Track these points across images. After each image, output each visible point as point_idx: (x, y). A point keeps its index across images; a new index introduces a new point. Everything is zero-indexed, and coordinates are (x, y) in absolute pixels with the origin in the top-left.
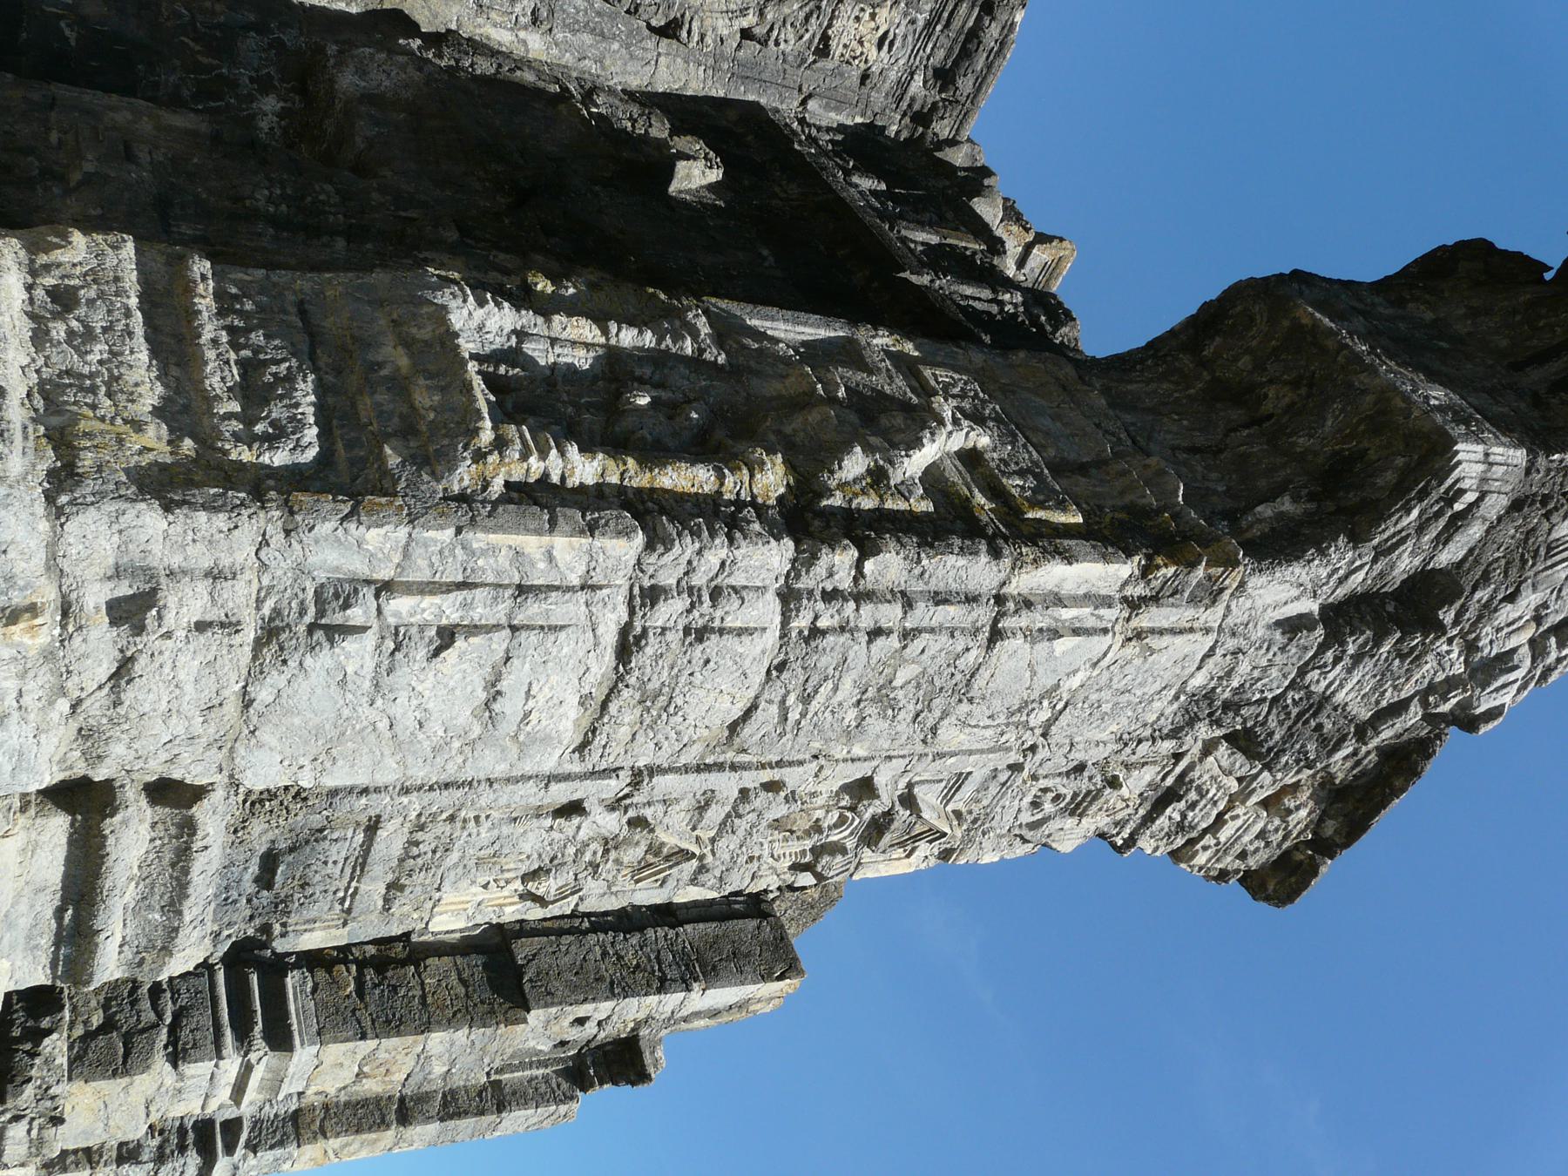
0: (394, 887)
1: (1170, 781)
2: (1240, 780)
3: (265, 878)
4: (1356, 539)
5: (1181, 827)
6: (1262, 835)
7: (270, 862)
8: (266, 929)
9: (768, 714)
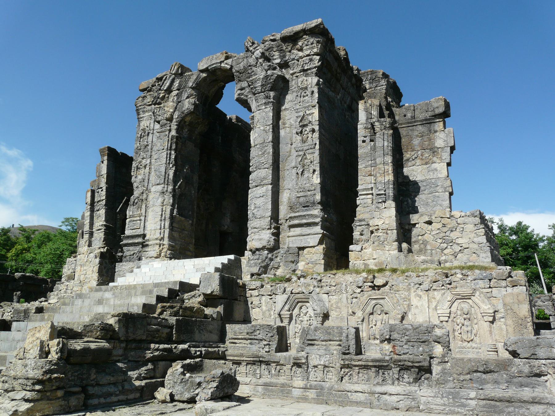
0: (309, 191)
1: (302, 73)
2: (298, 61)
3: (308, 206)
4: (247, 100)
5: (311, 60)
6: (307, 45)
7: (304, 207)
8: (318, 203)
9: (265, 166)
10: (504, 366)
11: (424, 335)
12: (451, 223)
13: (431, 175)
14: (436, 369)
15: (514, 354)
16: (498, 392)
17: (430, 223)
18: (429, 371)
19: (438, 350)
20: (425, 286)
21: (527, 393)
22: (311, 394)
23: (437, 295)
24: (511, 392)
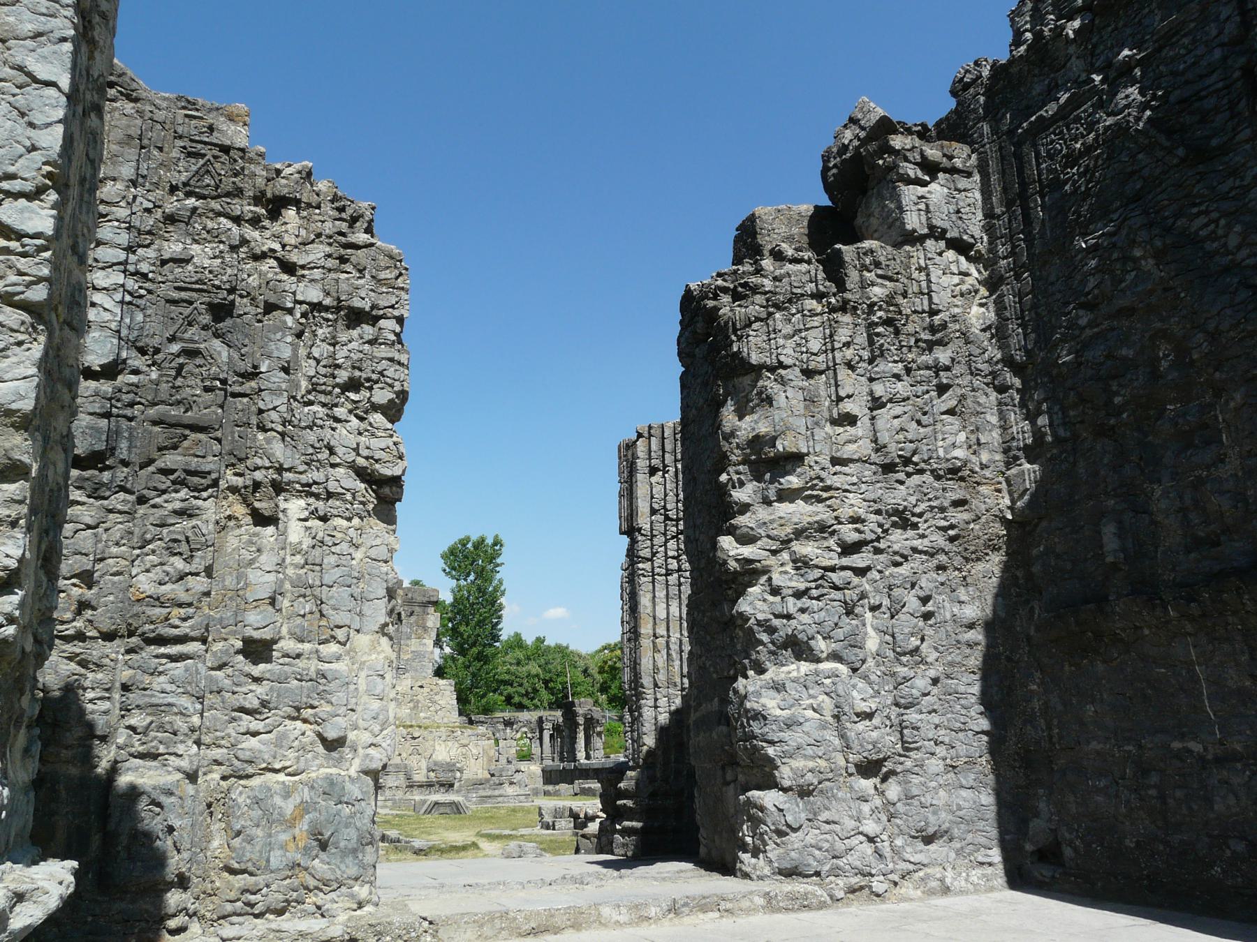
10: (487, 781)
11: (451, 767)
12: (436, 689)
13: (421, 648)
14: (457, 785)
15: (493, 775)
16: (485, 794)
17: (421, 687)
18: (452, 785)
19: (458, 774)
20: (444, 738)
21: (497, 793)
22: (389, 804)
23: (450, 744)
24: (489, 793)
